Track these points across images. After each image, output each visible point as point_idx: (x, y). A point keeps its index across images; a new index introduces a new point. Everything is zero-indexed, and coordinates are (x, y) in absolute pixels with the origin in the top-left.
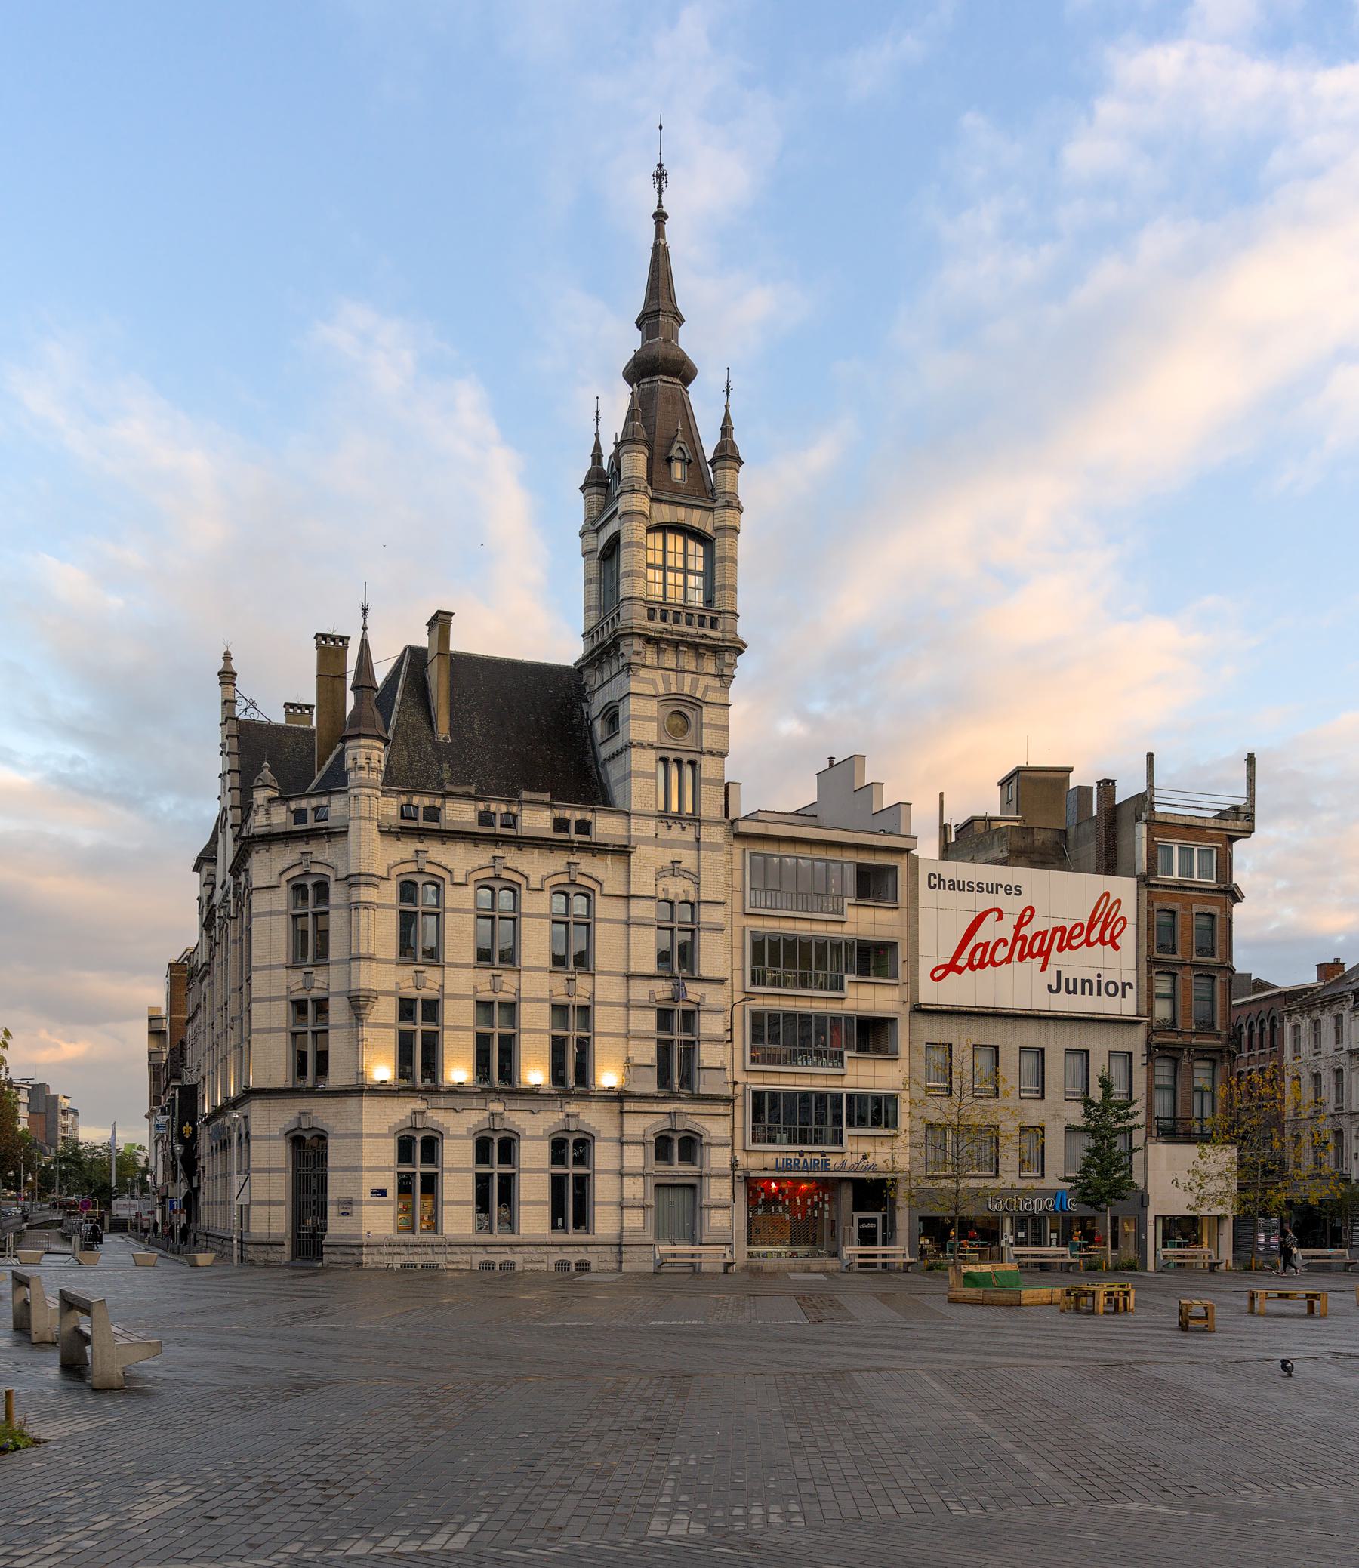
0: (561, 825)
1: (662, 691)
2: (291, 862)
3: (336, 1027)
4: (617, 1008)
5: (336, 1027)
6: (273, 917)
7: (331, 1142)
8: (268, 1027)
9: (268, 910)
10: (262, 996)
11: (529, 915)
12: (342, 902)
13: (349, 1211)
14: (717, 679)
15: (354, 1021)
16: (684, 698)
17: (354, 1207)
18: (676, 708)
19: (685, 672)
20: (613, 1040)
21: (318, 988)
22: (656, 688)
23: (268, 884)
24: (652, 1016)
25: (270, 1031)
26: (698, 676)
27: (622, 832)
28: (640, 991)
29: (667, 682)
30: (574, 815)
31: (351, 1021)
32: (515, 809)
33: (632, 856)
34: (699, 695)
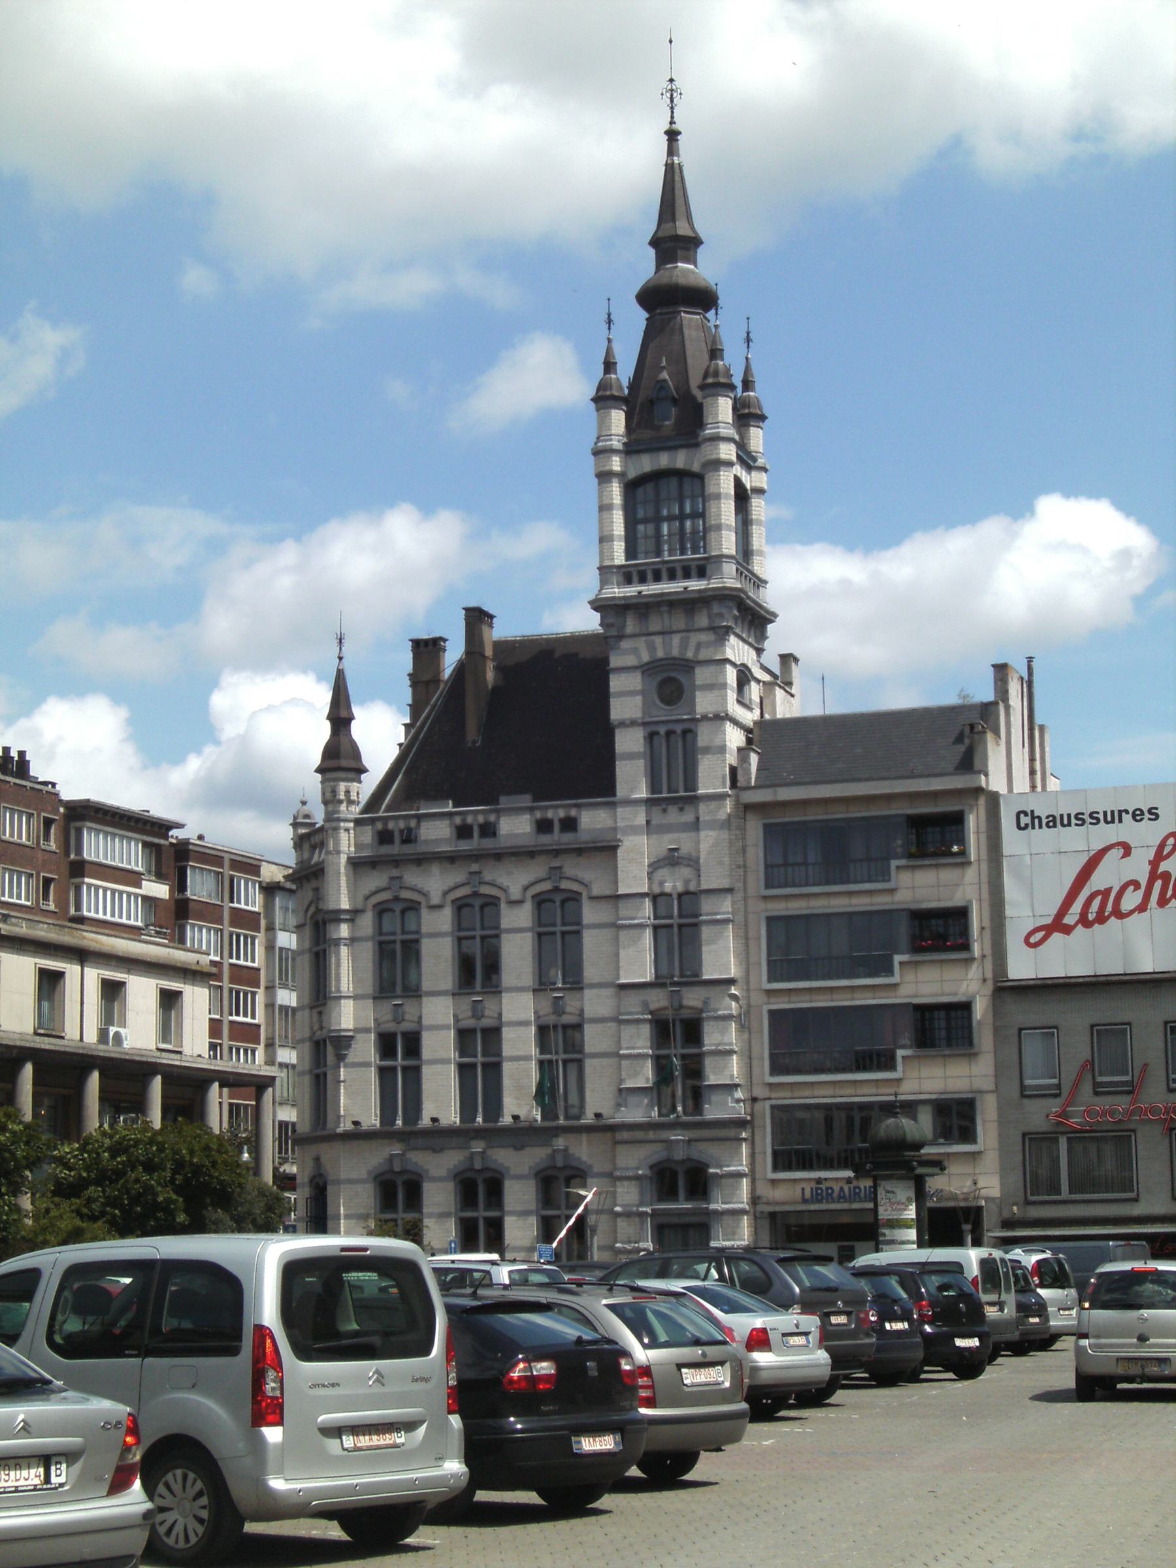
0: (543, 826)
1: (646, 657)
4: (609, 1024)
11: (510, 931)
14: (711, 632)
16: (671, 662)
18: (665, 675)
19: (671, 633)
20: (605, 1061)
22: (639, 657)
24: (646, 1030)
26: (688, 634)
27: (609, 823)
28: (633, 1004)
29: (651, 648)
30: (555, 812)
32: (492, 818)
33: (620, 852)
34: (690, 654)
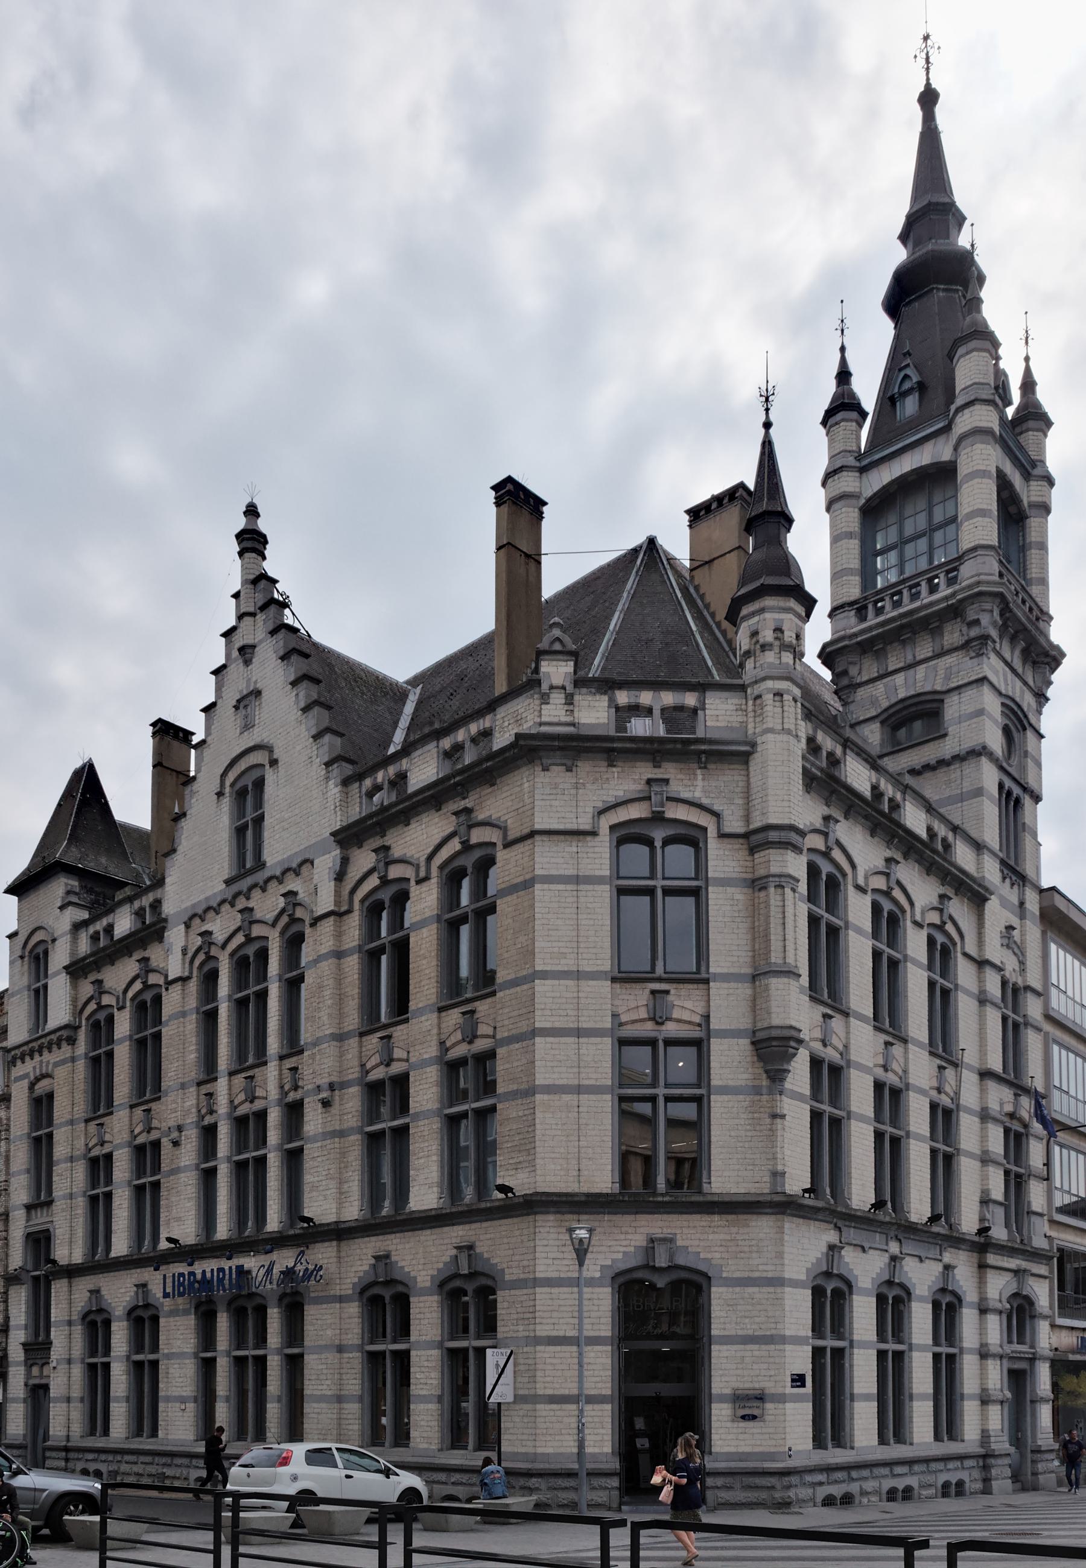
2: (621, 793)
3: (725, 1090)
5: (725, 1090)
6: (581, 887)
7: (719, 1297)
8: (576, 1082)
9: (571, 872)
10: (557, 1025)
12: (734, 875)
13: (756, 1412)
15: (765, 1083)
17: (769, 1406)
21: (679, 1021)
23: (573, 826)
25: (579, 1090)
31: (757, 1083)
